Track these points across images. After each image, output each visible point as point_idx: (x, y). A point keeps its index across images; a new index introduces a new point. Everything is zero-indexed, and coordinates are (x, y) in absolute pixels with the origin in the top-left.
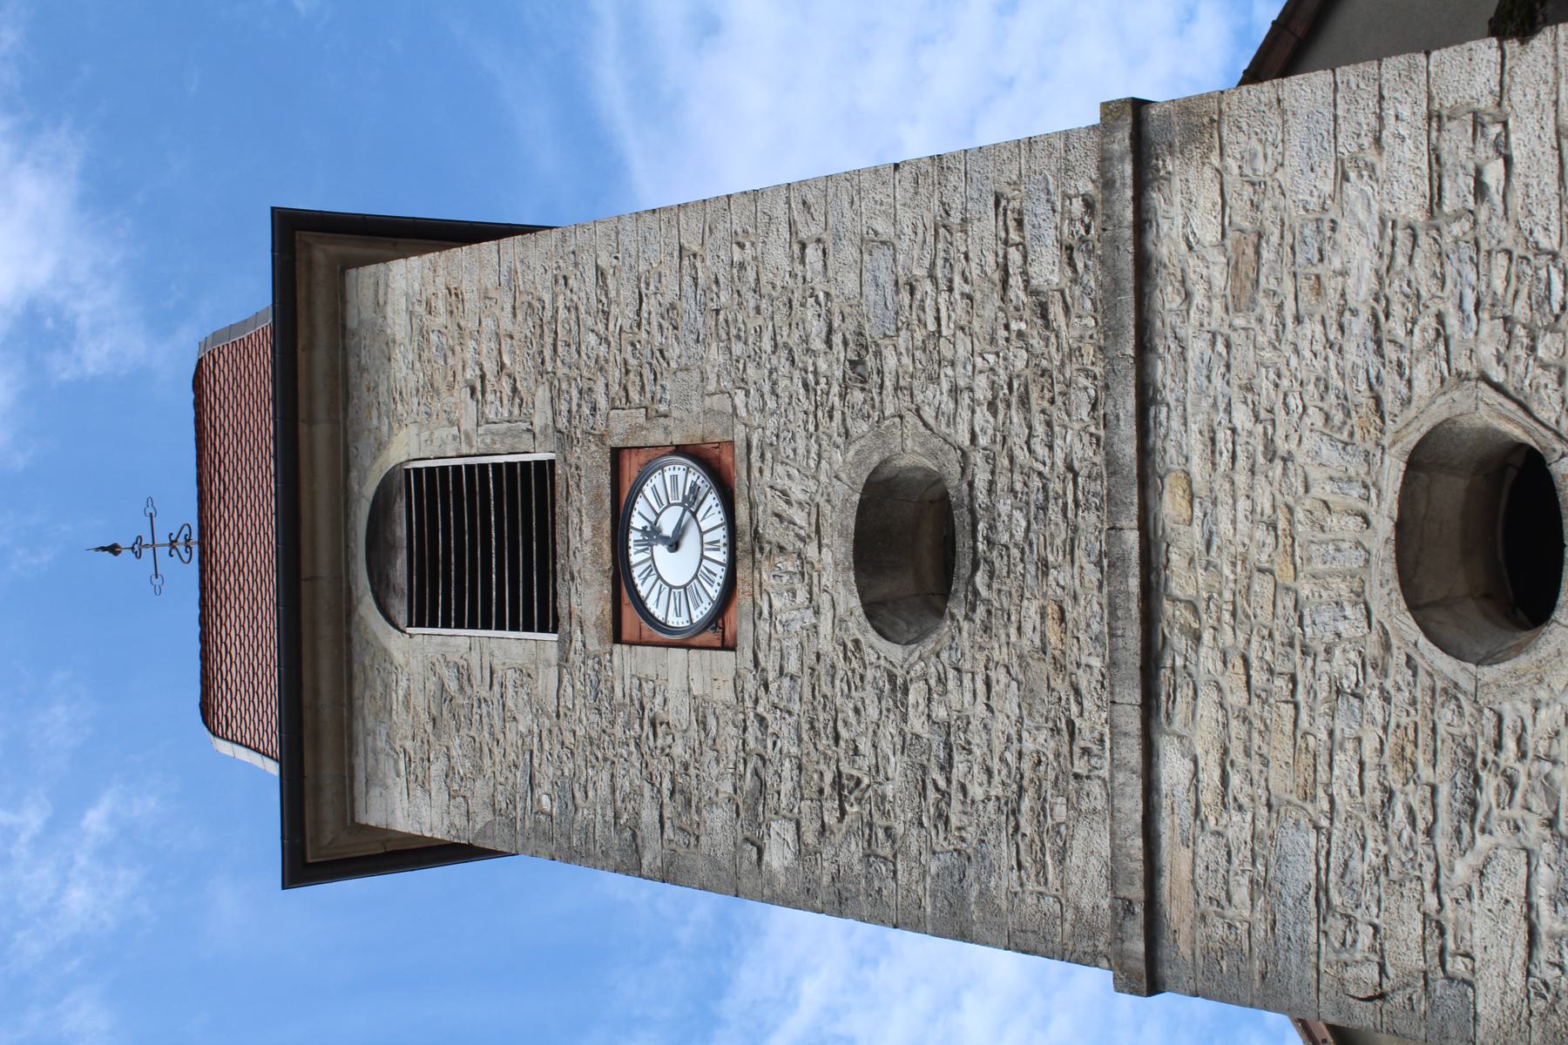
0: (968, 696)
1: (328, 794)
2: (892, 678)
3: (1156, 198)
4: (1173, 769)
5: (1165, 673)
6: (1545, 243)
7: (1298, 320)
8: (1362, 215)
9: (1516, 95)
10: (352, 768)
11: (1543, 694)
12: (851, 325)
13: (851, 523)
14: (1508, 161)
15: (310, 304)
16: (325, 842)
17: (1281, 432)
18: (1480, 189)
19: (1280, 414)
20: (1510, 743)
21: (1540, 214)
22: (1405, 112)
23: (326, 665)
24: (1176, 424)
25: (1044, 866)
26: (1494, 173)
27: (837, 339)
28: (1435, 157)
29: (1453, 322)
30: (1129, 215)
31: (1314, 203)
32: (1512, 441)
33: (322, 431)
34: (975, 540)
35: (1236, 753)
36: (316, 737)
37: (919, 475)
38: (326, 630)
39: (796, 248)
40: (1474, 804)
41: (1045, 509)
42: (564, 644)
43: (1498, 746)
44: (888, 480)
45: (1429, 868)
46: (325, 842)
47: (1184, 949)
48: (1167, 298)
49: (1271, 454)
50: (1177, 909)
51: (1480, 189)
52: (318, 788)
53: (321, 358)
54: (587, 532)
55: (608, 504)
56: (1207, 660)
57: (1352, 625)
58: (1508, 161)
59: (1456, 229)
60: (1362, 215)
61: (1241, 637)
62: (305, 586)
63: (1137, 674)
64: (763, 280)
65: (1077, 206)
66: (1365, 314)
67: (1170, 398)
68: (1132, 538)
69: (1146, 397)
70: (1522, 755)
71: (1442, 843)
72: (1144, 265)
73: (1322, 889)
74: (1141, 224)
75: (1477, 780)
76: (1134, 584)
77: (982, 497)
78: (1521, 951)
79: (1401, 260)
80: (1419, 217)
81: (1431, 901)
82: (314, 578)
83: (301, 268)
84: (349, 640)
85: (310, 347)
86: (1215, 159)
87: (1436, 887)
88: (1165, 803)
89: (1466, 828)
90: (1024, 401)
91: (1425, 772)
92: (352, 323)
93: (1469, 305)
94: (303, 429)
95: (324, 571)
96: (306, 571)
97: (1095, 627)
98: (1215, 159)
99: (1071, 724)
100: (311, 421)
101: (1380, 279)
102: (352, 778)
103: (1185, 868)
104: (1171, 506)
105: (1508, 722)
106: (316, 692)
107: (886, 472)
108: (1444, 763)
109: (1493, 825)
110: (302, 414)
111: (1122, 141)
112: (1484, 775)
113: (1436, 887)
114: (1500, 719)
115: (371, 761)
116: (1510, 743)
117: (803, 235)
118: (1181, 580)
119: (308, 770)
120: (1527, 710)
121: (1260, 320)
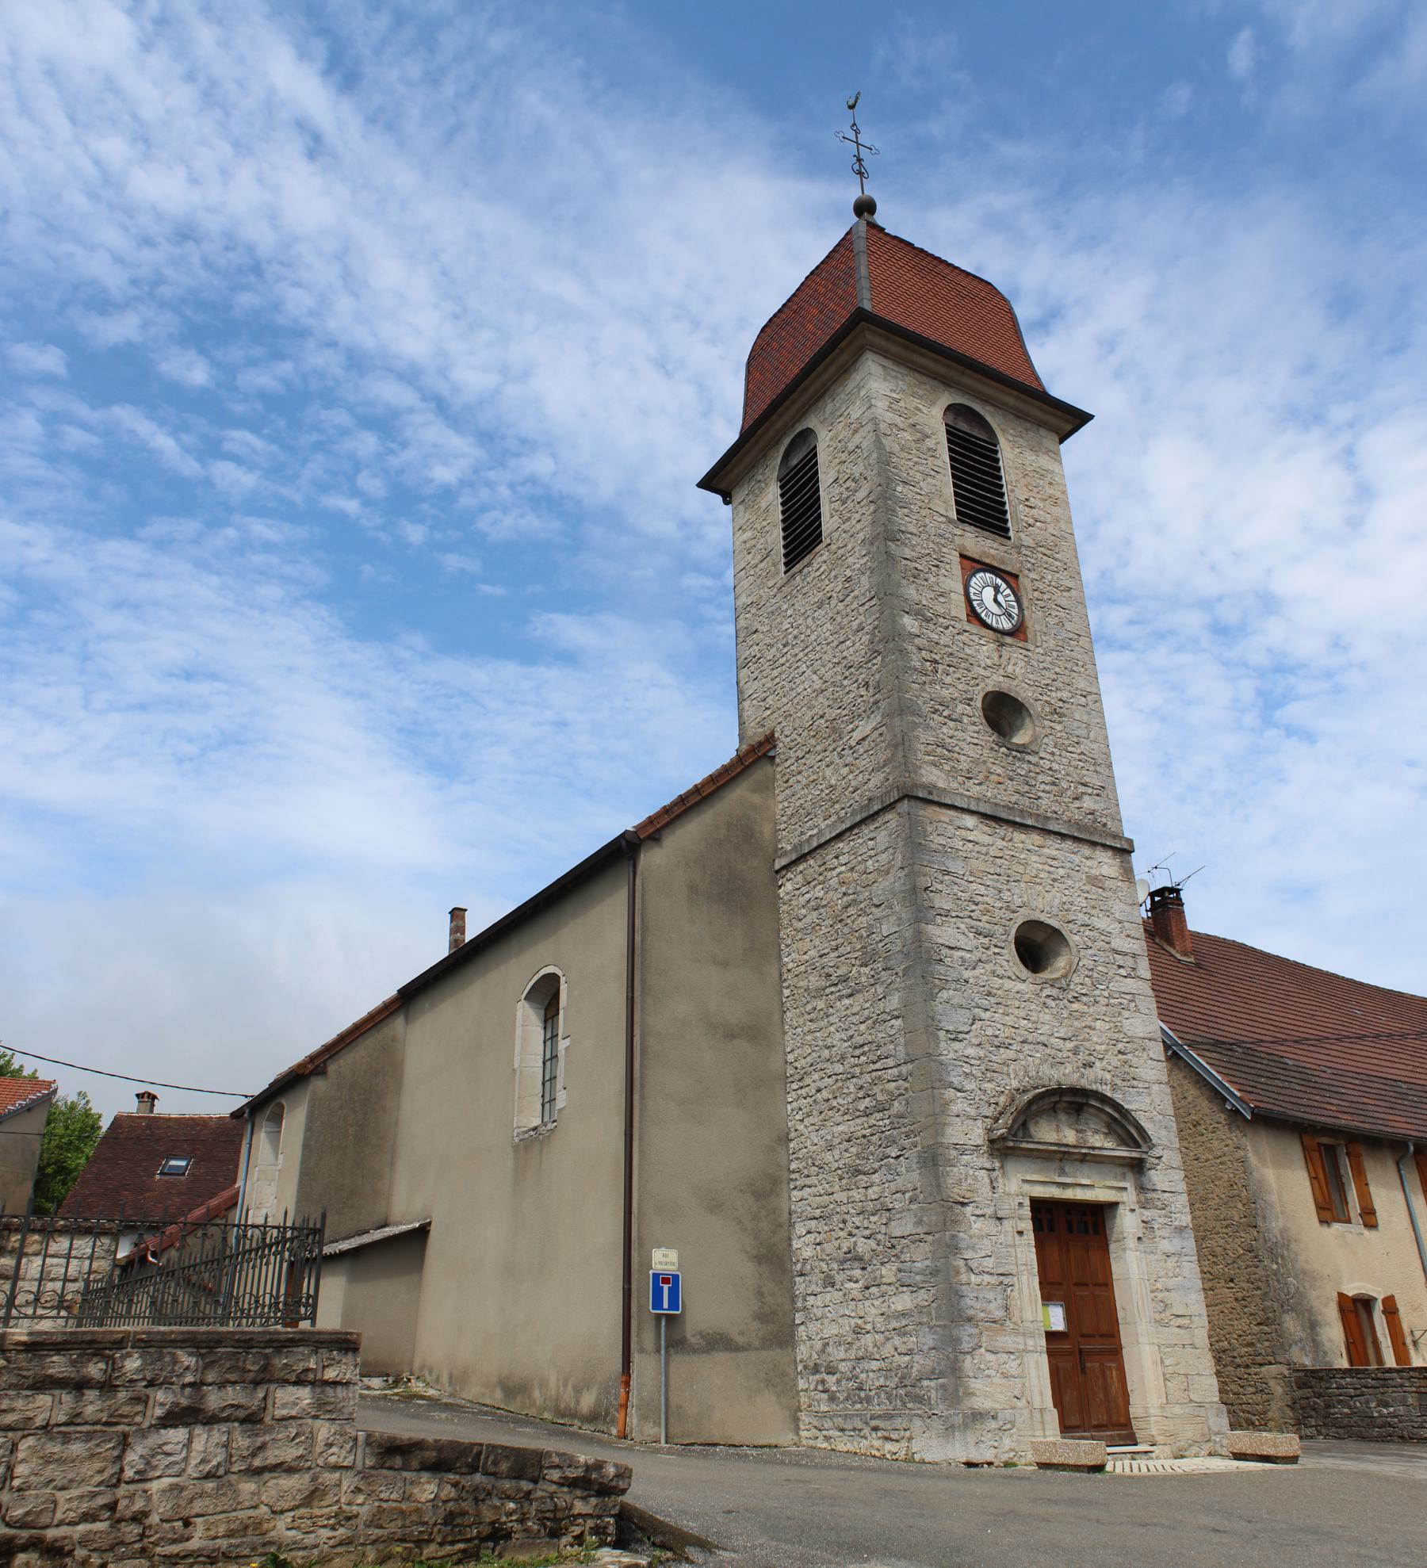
0: (972, 734)
1: (884, 343)
2: (971, 699)
3: (1110, 853)
4: (970, 821)
5: (994, 825)
6: (1111, 985)
7: (1086, 898)
8: (1112, 926)
9: (1140, 983)
10: (888, 358)
11: (1011, 964)
12: (1066, 712)
13: (1012, 694)
14: (1126, 977)
15: (1055, 415)
16: (866, 332)
17: (1060, 885)
18: (1120, 967)
19: (1064, 886)
20: (997, 950)
21: (1116, 985)
22: (1135, 946)
23: (931, 365)
24: (1057, 846)
25: (929, 755)
26: (1122, 972)
27: (1061, 704)
28: (1126, 954)
29: (1090, 952)
30: (1108, 843)
31: (1113, 911)
32: (1049, 959)
33: (1011, 401)
34: (1017, 751)
35: (977, 848)
36: (906, 347)
37: (1018, 723)
38: (943, 370)
39: (1084, 693)
40: (980, 934)
41: (1027, 784)
42: (950, 521)
43: (996, 946)
44: (1021, 712)
45: (961, 915)
46: (866, 332)
47: (921, 812)
48: (1086, 850)
49: (1054, 880)
50: (930, 811)
51: (1120, 967)
52: (888, 339)
53: (1036, 412)
54: (993, 552)
55: (1002, 567)
56: (1000, 843)
57: (1018, 902)
58: (1126, 977)
59: (1111, 958)
60: (1112, 926)
61: (1007, 857)
62: (962, 368)
63: (994, 814)
64: (1075, 674)
65: (1104, 820)
66: (1089, 922)
67: (1063, 845)
68: (1029, 822)
69: (1063, 836)
70: (995, 954)
71: (967, 920)
72: (1094, 844)
73: (948, 873)
74: (1104, 846)
75: (986, 937)
76: (1018, 819)
77: (1027, 757)
78: (947, 944)
79: (1103, 937)
80: (1113, 945)
81: (954, 914)
82: (963, 373)
83: (1068, 417)
84: (934, 379)
85: (1042, 410)
86: (1120, 878)
87: (957, 916)
88: (959, 815)
89: (974, 930)
90: (1054, 784)
91: (984, 918)
92: (1043, 432)
93: (1095, 958)
94: (1016, 393)
95: (965, 380)
96: (968, 372)
97: (999, 796)
98: (1120, 878)
99: (970, 778)
100: (1017, 398)
101: (1098, 929)
102: (885, 357)
103: (943, 819)
104: (1036, 838)
105: (1003, 951)
106: (923, 355)
107: (1024, 713)
108: (987, 926)
109: (976, 941)
110: (1022, 396)
111: (1126, 846)
112: (987, 939)
113: (957, 916)
114: (1003, 948)
115: (894, 374)
116: (997, 950)
117: (1089, 697)
118: (1019, 836)
119: (897, 339)
120: (1006, 957)
121: (1085, 885)
